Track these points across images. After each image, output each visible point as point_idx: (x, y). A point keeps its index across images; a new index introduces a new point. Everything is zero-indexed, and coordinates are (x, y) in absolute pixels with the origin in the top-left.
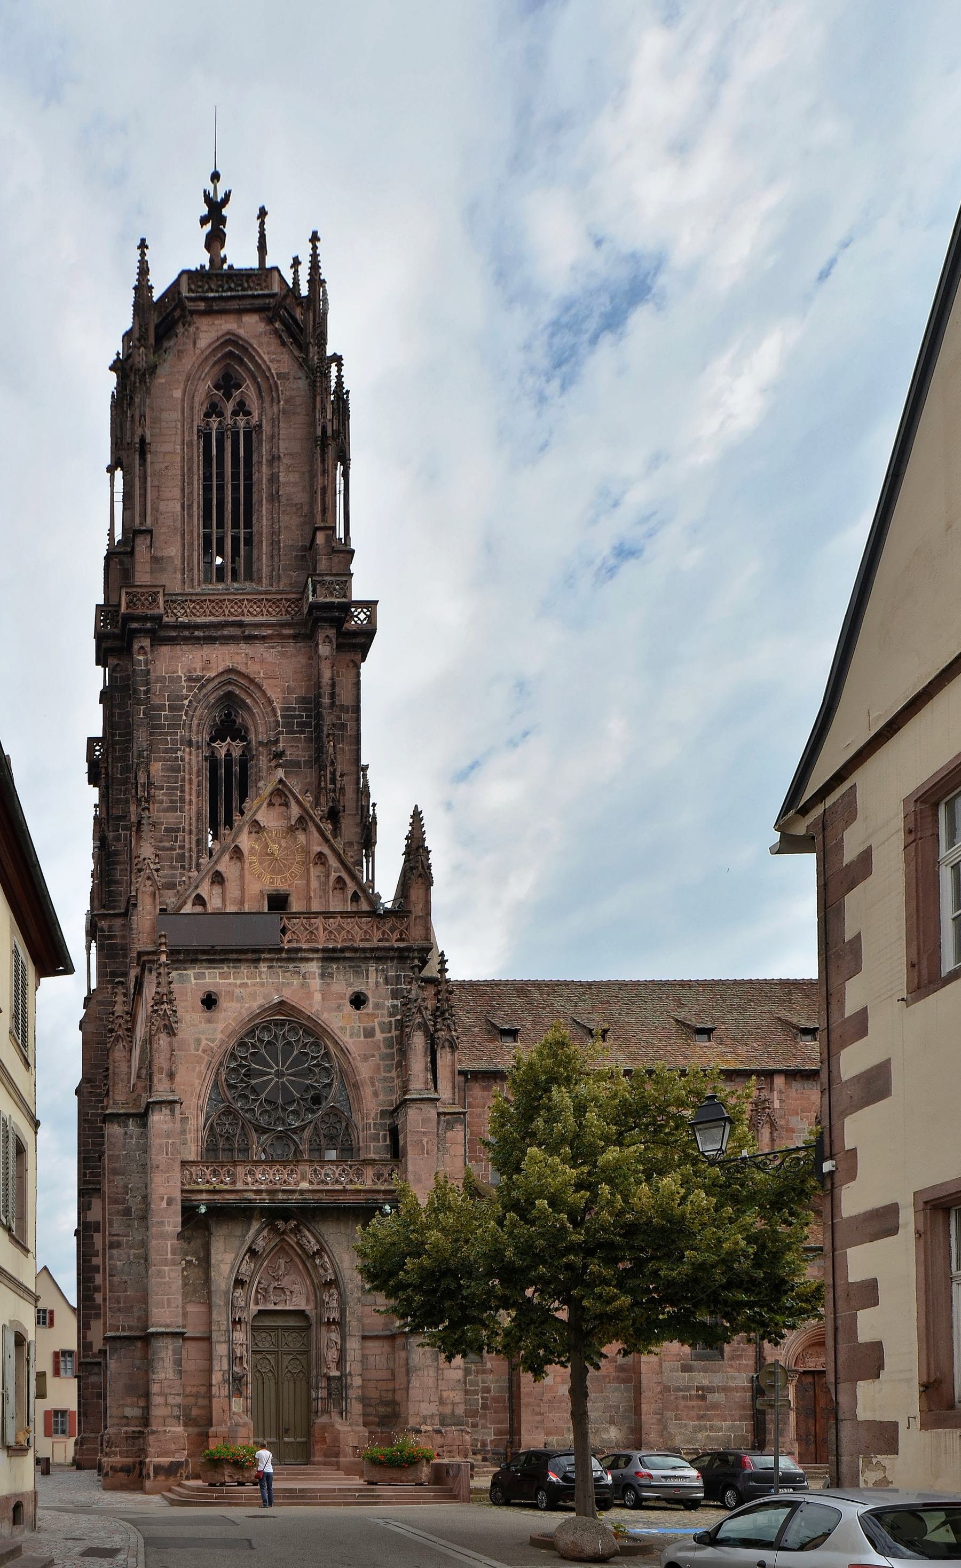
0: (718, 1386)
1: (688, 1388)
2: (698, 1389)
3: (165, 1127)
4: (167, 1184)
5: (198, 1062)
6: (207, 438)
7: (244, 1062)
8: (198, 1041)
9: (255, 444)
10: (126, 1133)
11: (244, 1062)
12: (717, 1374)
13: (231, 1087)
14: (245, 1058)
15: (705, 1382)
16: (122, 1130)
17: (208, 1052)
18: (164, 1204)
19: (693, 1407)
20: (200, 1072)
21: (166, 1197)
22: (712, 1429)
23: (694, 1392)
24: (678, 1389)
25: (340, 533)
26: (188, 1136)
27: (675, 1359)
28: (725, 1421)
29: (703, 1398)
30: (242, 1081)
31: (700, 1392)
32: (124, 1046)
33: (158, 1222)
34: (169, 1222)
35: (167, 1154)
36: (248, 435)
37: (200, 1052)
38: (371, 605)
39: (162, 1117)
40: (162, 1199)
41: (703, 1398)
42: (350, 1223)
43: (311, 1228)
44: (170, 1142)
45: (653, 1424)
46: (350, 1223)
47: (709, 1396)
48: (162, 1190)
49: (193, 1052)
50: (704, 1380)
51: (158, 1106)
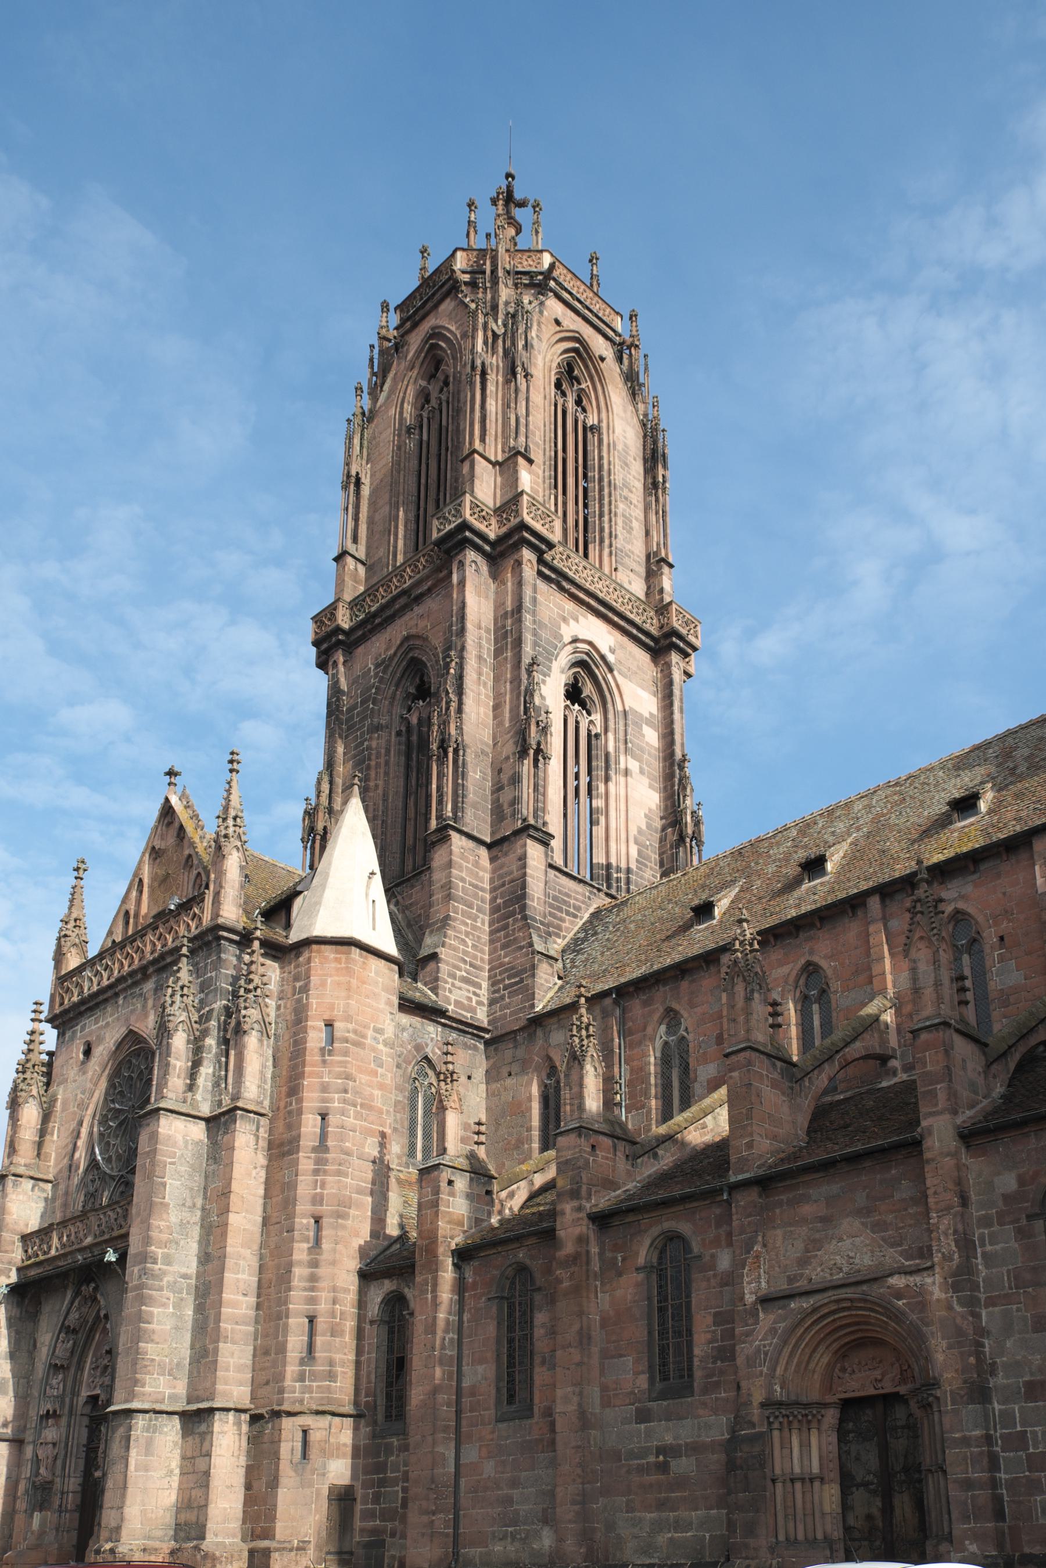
0: (687, 1444)
1: (644, 1453)
2: (660, 1450)
12: (684, 1422)
15: (669, 1439)
19: (651, 1485)
22: (677, 1526)
23: (652, 1459)
24: (632, 1455)
27: (627, 1401)
28: (696, 1509)
29: (663, 1468)
31: (661, 1458)
41: (663, 1468)
45: (570, 1521)
47: (673, 1463)
50: (667, 1434)
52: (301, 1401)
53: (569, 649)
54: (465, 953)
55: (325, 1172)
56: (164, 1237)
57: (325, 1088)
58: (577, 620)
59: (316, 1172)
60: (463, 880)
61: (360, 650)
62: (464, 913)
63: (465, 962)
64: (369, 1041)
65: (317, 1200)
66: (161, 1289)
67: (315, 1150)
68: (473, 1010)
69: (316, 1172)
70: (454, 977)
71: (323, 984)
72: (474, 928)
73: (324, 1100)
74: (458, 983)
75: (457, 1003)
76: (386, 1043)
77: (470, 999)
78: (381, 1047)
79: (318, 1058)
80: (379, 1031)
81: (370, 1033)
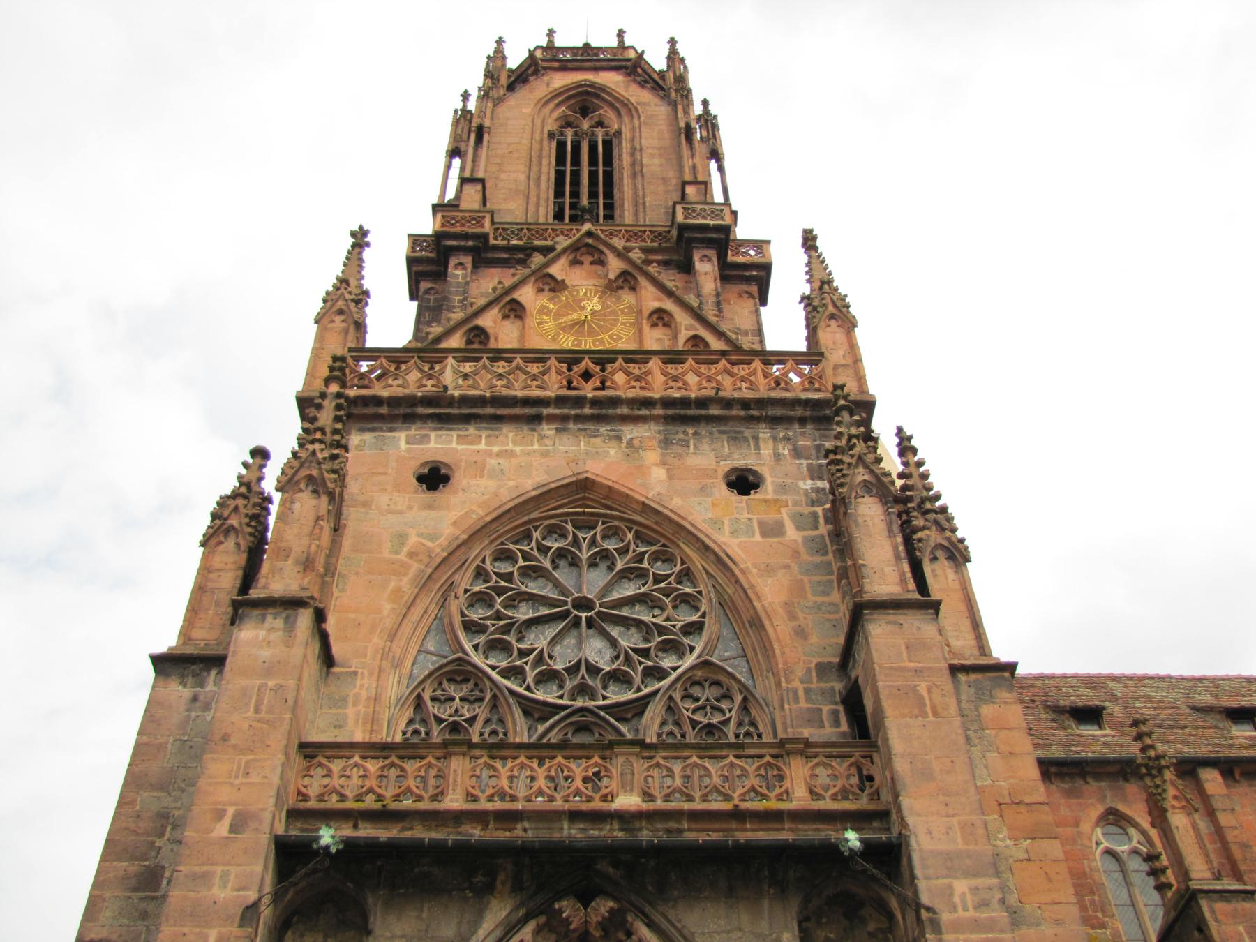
3: (265, 653)
4: (241, 780)
5: (395, 573)
6: (561, 146)
7: (503, 584)
8: (401, 538)
9: (615, 152)
10: (195, 699)
11: (503, 584)
13: (470, 627)
14: (508, 577)
16: (187, 692)
17: (420, 557)
18: (222, 829)
20: (398, 591)
21: (231, 811)
25: (718, 197)
26: (350, 711)
30: (498, 616)
32: (238, 544)
33: (194, 877)
34: (225, 877)
35: (257, 711)
36: (608, 144)
37: (402, 556)
38: (760, 245)
39: (262, 634)
40: (220, 815)
42: (766, 903)
43: (658, 918)
44: (271, 683)
46: (766, 903)
48: (224, 794)
49: (387, 554)
51: (256, 612)
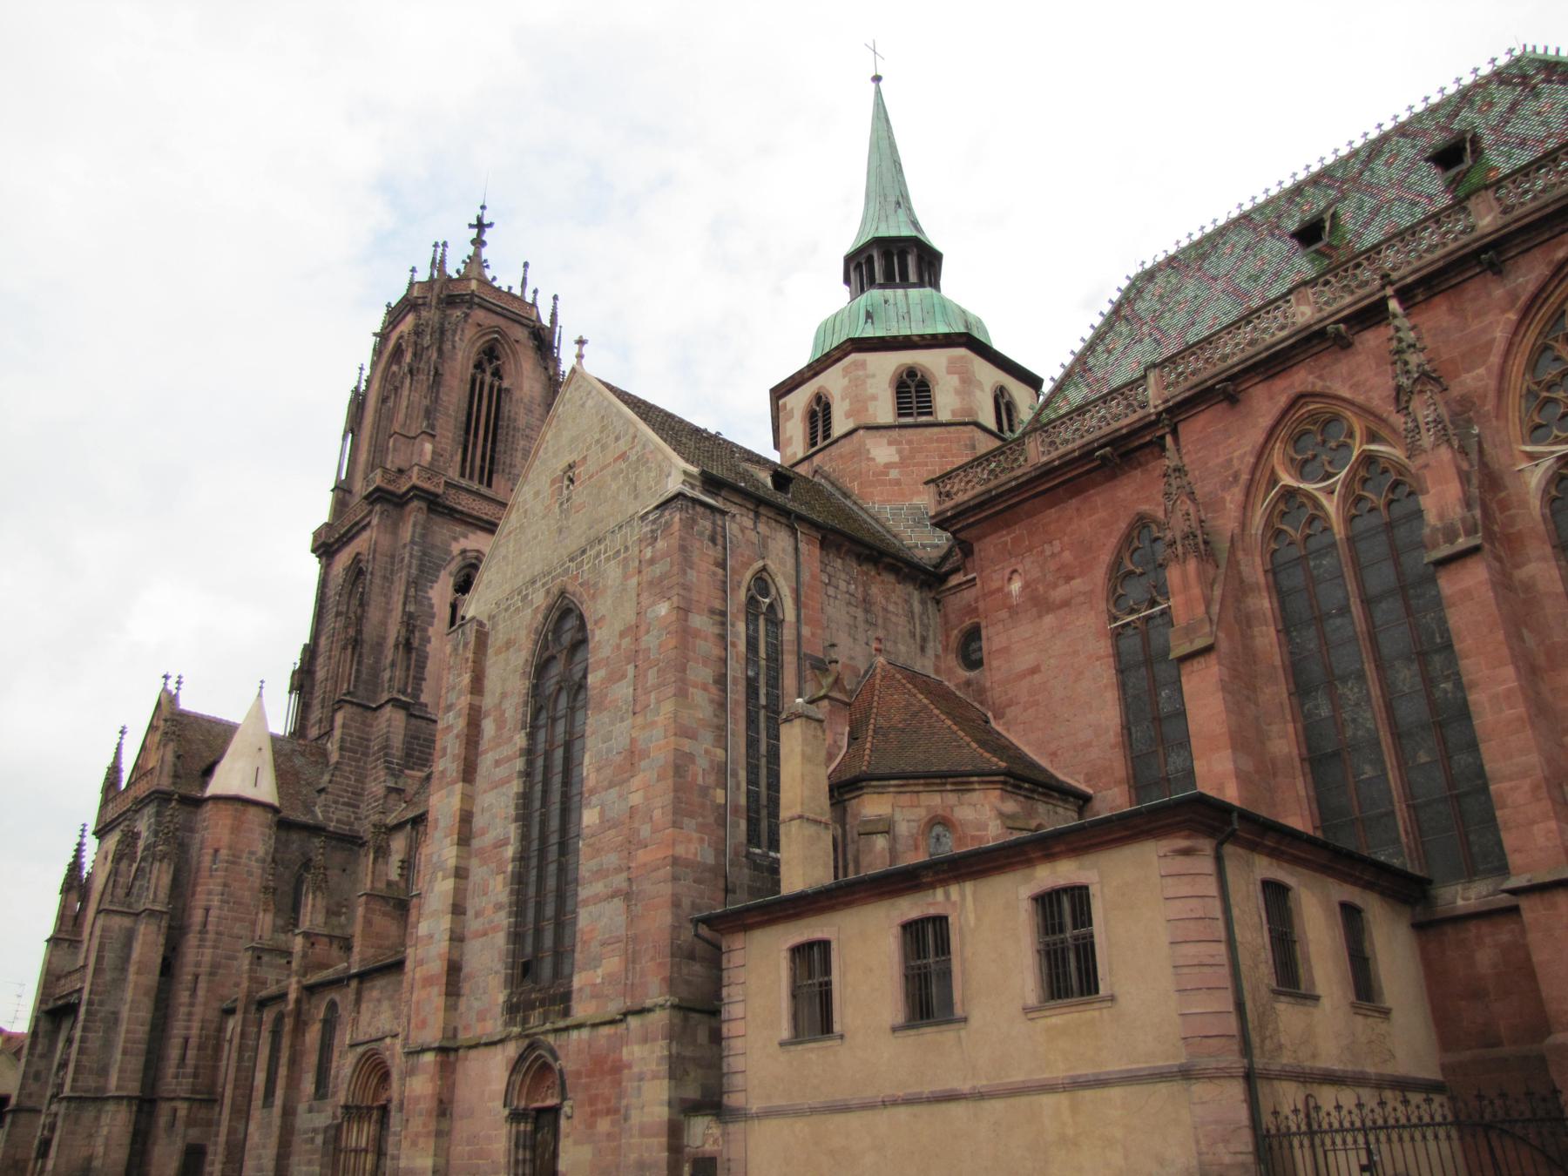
52: (174, 1091)
53: (460, 558)
54: (348, 785)
55: (204, 947)
56: (100, 989)
57: (210, 893)
58: (466, 537)
59: (199, 947)
60: (351, 735)
61: (338, 557)
62: (349, 758)
63: (347, 791)
64: (244, 860)
65: (198, 964)
66: (95, 1021)
67: (200, 932)
68: (351, 824)
69: (199, 947)
70: (336, 802)
71: (217, 824)
72: (358, 767)
73: (208, 900)
74: (340, 807)
75: (338, 821)
76: (257, 861)
77: (349, 817)
78: (253, 863)
79: (207, 874)
80: (252, 853)
81: (245, 856)
